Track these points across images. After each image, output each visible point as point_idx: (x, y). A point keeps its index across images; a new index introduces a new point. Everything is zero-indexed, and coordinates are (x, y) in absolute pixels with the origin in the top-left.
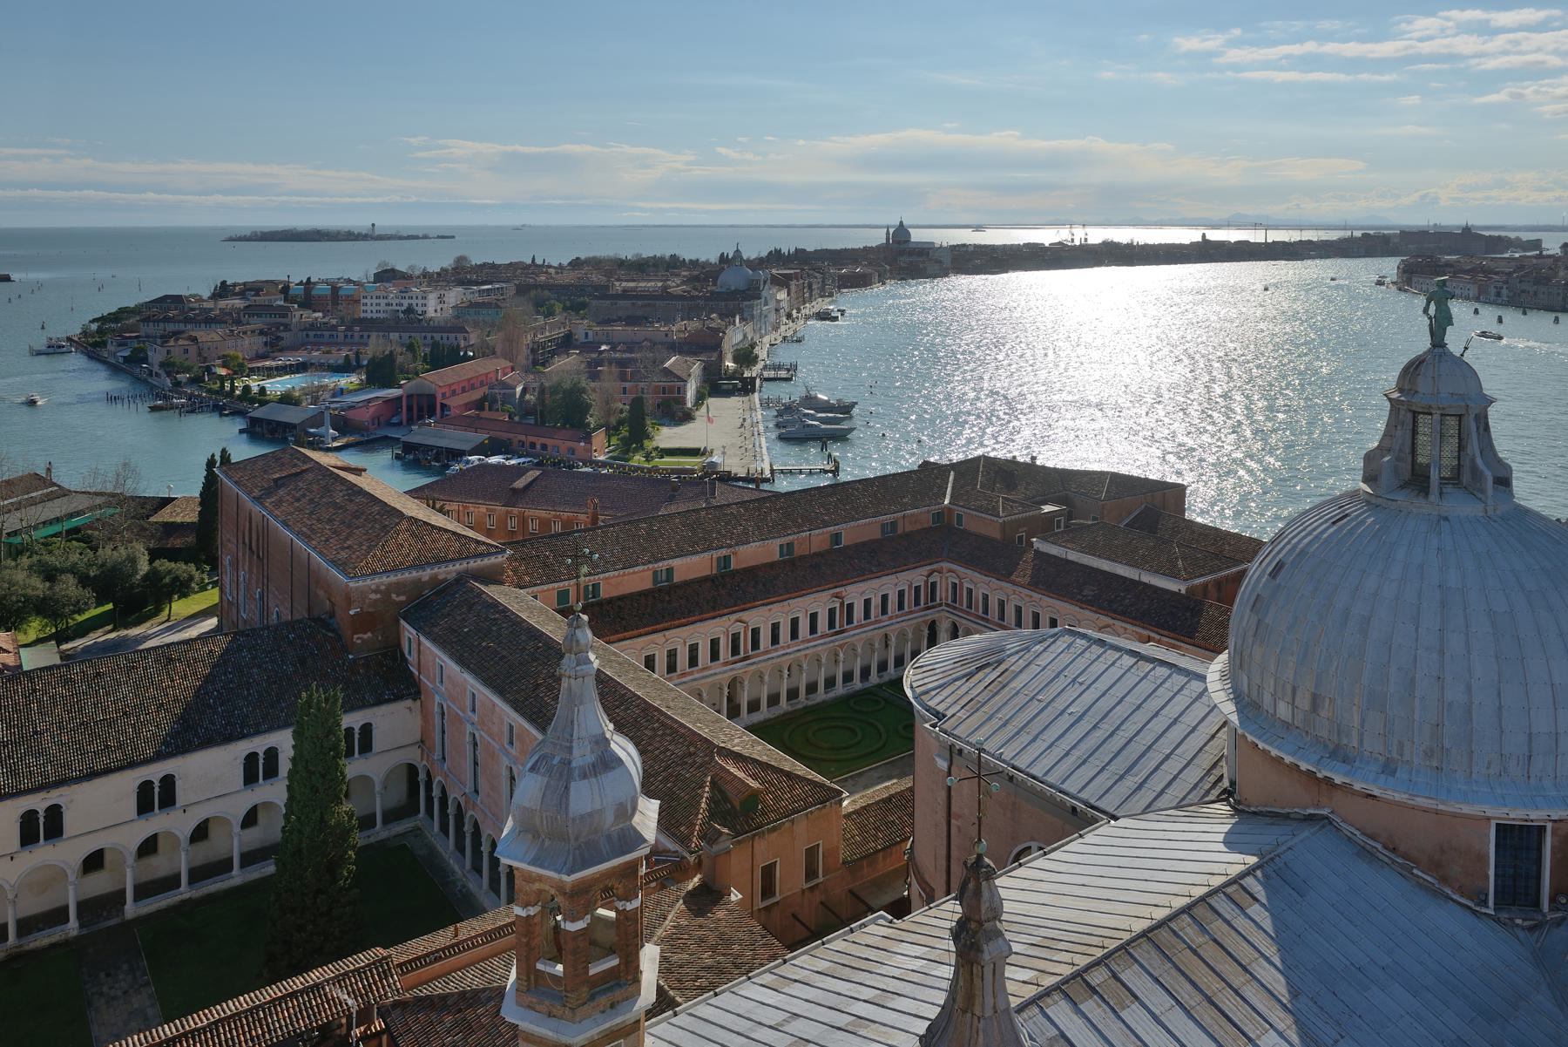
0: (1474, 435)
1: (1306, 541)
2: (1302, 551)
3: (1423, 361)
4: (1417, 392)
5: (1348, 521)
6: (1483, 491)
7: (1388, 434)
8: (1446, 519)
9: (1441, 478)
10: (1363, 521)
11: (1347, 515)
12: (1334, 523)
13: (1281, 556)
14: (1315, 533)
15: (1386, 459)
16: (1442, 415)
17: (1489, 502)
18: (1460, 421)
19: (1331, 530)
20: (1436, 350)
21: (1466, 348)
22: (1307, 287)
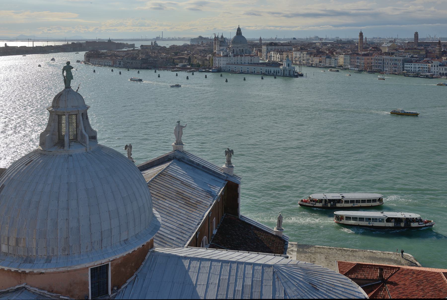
0: (82, 122)
1: (14, 174)
2: (13, 179)
3: (62, 94)
4: (59, 107)
5: (32, 163)
6: (85, 142)
7: (49, 125)
8: (71, 156)
9: (70, 140)
10: (38, 162)
11: (32, 161)
12: (26, 165)
13: (3, 182)
14: (18, 170)
15: (48, 135)
16: (69, 115)
17: (88, 146)
18: (76, 116)
19: (25, 168)
20: (67, 90)
21: (78, 88)
22: (10, 68)
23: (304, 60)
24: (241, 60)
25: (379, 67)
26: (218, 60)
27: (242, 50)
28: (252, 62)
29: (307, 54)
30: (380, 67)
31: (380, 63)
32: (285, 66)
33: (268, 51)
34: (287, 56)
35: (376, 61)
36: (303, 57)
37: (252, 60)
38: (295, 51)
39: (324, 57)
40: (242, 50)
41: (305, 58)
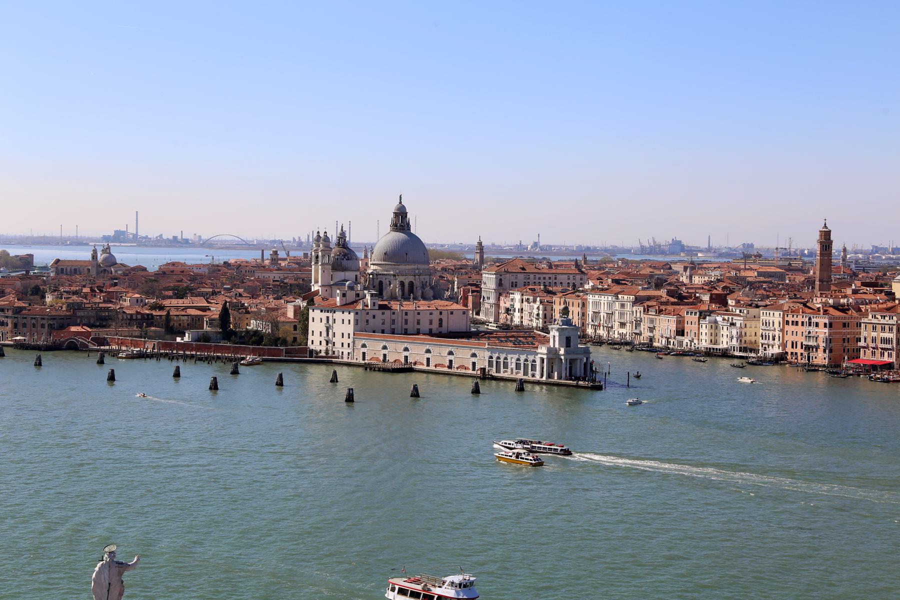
23: (623, 325)
24: (406, 321)
25: (882, 355)
26: (324, 321)
27: (411, 284)
28: (444, 330)
29: (634, 303)
30: (886, 354)
31: (886, 341)
32: (557, 346)
33: (502, 289)
34: (565, 311)
35: (874, 334)
36: (622, 315)
37: (444, 324)
38: (594, 289)
39: (691, 319)
40: (411, 284)
41: (627, 318)
